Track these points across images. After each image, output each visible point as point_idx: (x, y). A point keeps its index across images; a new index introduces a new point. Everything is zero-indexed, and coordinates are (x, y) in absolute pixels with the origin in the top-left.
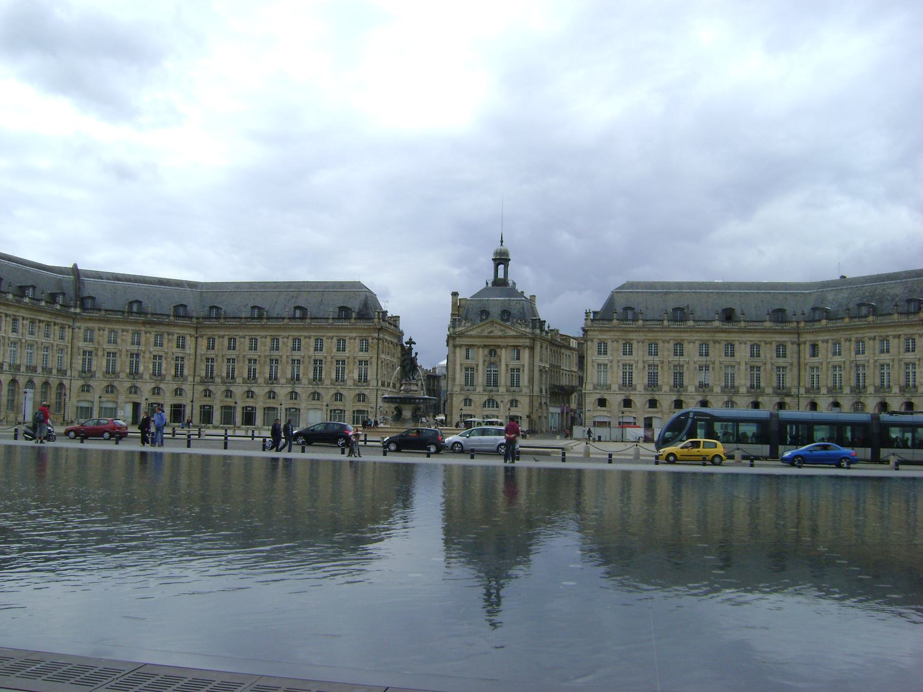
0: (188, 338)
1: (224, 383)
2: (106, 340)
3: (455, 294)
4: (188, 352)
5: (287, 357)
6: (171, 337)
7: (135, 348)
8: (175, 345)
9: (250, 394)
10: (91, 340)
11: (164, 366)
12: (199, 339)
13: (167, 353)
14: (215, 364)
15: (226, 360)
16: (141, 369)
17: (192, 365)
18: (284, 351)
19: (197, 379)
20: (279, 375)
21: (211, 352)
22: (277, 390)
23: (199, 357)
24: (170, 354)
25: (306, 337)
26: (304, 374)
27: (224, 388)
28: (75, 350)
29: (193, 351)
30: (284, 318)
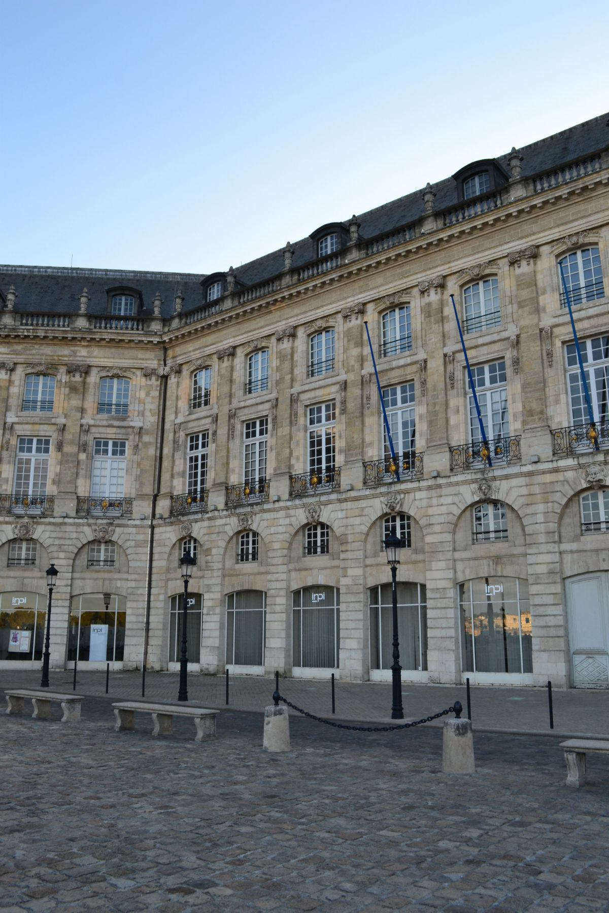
1: (232, 505)
4: (137, 423)
5: (448, 359)
6: (78, 378)
8: (90, 404)
9: (316, 538)
11: (53, 469)
12: (173, 380)
13: (63, 428)
15: (240, 429)
17: (149, 465)
18: (434, 339)
19: (164, 506)
20: (420, 444)
21: (202, 411)
22: (416, 500)
23: (169, 436)
24: (73, 429)
26: (529, 413)
27: (232, 524)
29: (151, 420)
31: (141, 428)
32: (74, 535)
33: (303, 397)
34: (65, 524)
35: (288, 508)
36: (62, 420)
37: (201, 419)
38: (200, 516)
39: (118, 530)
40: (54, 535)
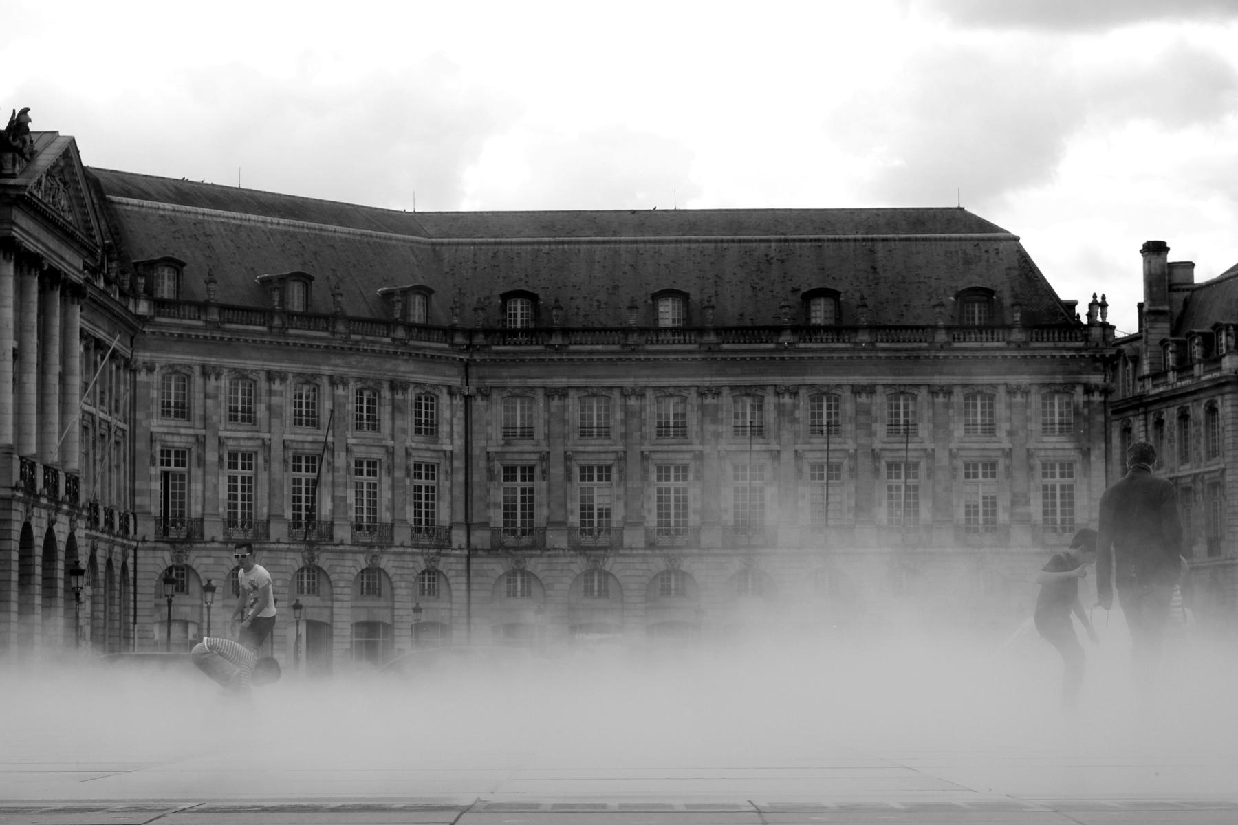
0: (444, 399)
2: (224, 411)
3: (1155, 249)
4: (448, 448)
7: (305, 437)
10: (182, 412)
11: (385, 495)
12: (479, 402)
13: (391, 452)
14: (540, 485)
15: (576, 471)
16: (325, 508)
17: (459, 492)
19: (481, 538)
23: (480, 464)
24: (400, 453)
25: (856, 390)
28: (141, 445)
29: (459, 442)
30: (778, 330)
31: (452, 452)
32: (411, 565)
33: (654, 456)
34: (404, 553)
35: (646, 555)
36: (390, 443)
37: (524, 451)
38: (539, 552)
39: (443, 560)
40: (396, 564)
